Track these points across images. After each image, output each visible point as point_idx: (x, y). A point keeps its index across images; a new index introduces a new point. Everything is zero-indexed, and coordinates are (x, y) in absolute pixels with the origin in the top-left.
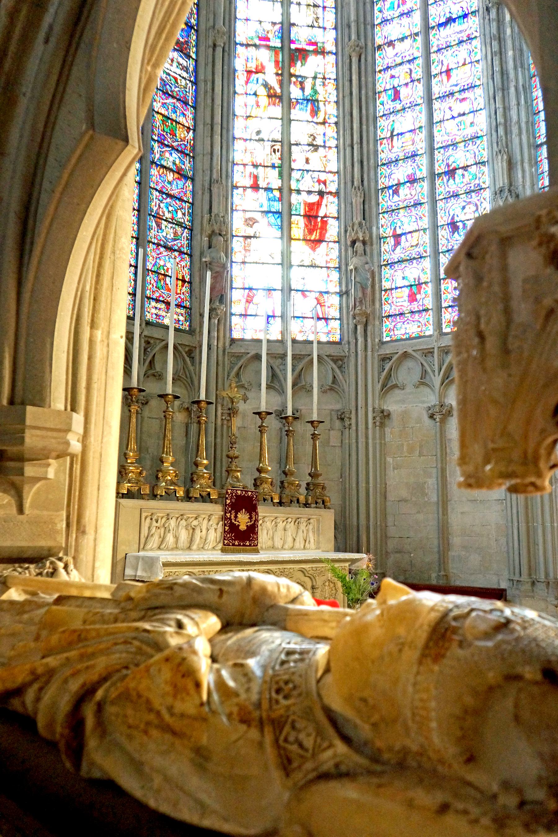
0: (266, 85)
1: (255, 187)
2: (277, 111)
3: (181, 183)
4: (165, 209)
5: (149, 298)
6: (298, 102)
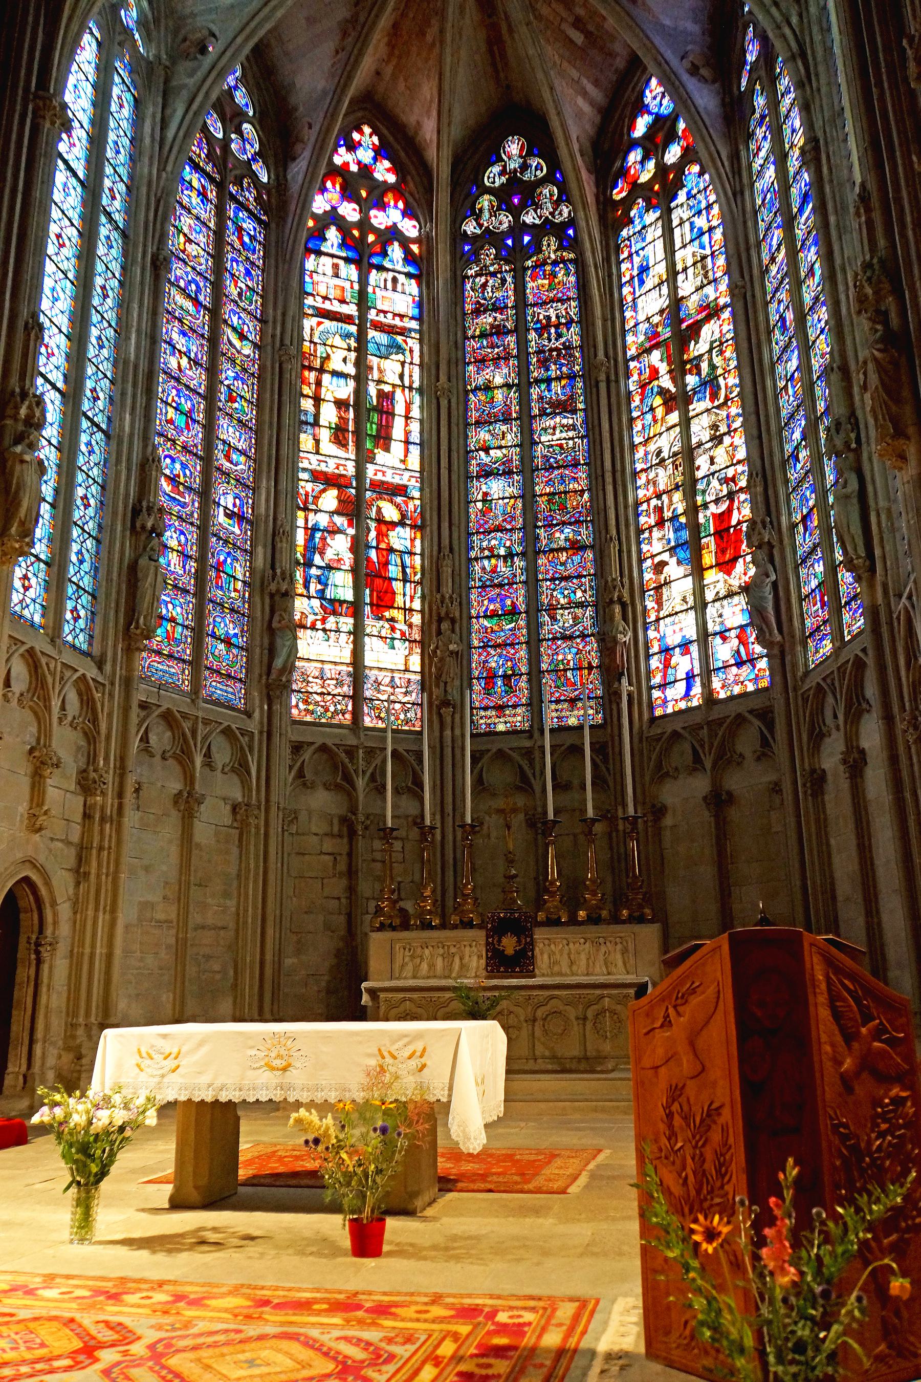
0: (662, 392)
1: (660, 523)
2: (674, 417)
3: (577, 559)
6: (695, 393)
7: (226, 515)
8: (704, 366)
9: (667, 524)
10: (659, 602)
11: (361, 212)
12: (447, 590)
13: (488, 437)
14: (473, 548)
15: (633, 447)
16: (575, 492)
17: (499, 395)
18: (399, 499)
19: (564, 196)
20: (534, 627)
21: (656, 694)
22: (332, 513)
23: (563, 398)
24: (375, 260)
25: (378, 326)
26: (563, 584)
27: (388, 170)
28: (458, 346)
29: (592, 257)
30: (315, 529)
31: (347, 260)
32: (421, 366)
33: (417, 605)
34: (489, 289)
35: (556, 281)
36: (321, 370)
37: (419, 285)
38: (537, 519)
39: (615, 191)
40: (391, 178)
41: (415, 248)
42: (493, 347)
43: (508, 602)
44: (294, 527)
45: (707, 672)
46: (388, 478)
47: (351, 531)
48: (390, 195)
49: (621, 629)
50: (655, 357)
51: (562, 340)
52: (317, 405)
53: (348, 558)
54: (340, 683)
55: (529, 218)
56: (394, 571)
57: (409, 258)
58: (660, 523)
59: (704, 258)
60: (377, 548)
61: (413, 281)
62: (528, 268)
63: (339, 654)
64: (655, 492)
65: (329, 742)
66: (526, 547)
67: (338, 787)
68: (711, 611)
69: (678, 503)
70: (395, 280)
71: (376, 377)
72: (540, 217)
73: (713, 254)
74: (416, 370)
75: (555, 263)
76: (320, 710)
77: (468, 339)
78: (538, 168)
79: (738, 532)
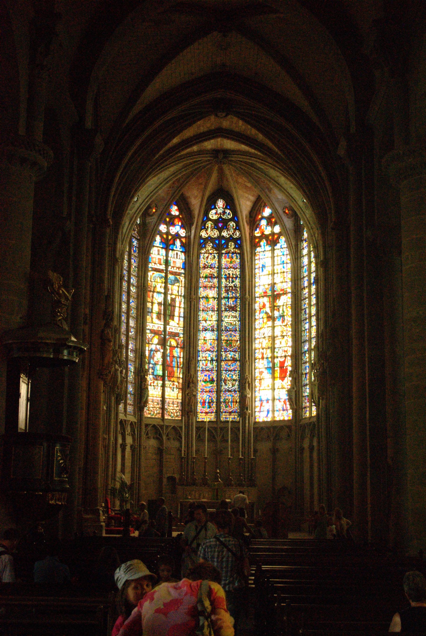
0: (266, 313)
1: (263, 358)
2: (270, 323)
4: (228, 377)
5: (222, 412)
7: (130, 351)
8: (281, 309)
9: (265, 359)
10: (260, 384)
11: (167, 229)
12: (192, 373)
13: (206, 316)
14: (199, 356)
15: (255, 329)
16: (235, 340)
17: (211, 300)
18: (177, 338)
19: (238, 228)
20: (219, 386)
21: (257, 414)
22: (156, 344)
23: (233, 306)
24: (171, 247)
25: (172, 273)
26: (229, 372)
27: (176, 210)
28: (197, 281)
29: (247, 257)
30: (151, 350)
31: (162, 248)
32: (185, 287)
33: (181, 376)
34: (209, 259)
35: (233, 260)
36: (154, 292)
37: (185, 256)
38: (222, 349)
39: (256, 232)
40: (177, 213)
41: (184, 240)
42: (209, 282)
43: (211, 377)
44: (146, 350)
45: (273, 411)
46: (173, 331)
47: (162, 351)
48: (177, 220)
49: (248, 392)
50: (266, 300)
51: (234, 283)
52: (152, 305)
53: (161, 360)
54: (158, 404)
55: (225, 234)
56: (174, 364)
57: (183, 245)
58: (263, 358)
59: (284, 272)
60: (169, 356)
61: (183, 254)
62: (223, 253)
63: (158, 394)
64: (262, 347)
65: (156, 424)
66: (218, 358)
67: (157, 438)
68: (276, 391)
69: (269, 353)
70: (177, 254)
71: (170, 293)
72: (229, 234)
73: (287, 272)
74: (183, 289)
75: (233, 253)
76: (152, 413)
77: (201, 278)
78: (229, 214)
79: (287, 369)
